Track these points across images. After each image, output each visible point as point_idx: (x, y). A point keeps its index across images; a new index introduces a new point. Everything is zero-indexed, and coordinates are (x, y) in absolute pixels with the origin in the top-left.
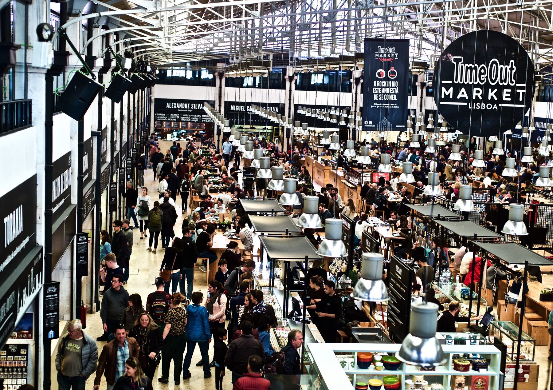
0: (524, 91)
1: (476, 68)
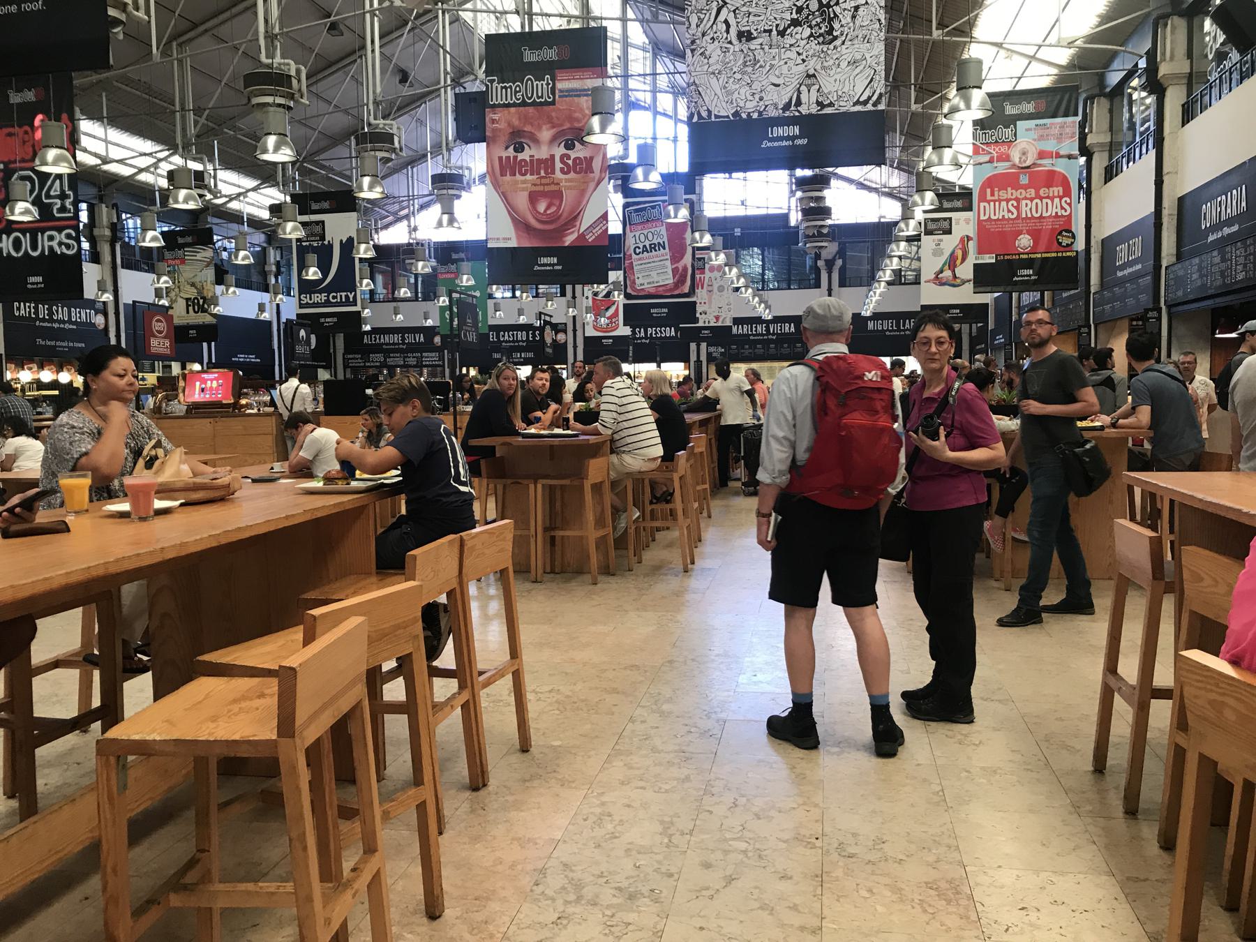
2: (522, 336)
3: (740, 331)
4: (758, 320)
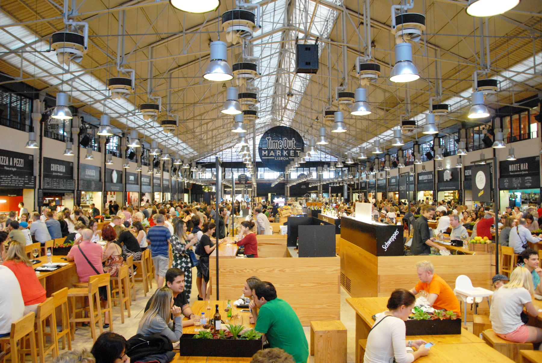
1: (277, 142)
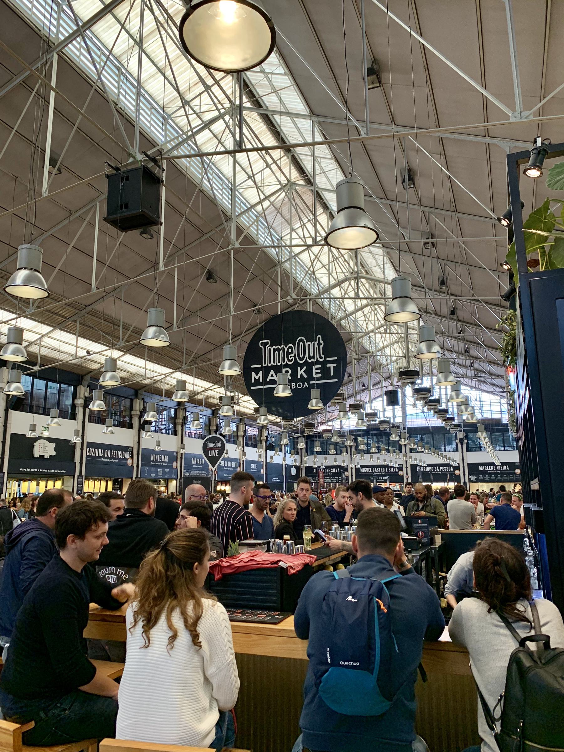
0: (335, 365)
1: (283, 349)
2: (382, 470)
3: (483, 469)
4: (493, 464)
